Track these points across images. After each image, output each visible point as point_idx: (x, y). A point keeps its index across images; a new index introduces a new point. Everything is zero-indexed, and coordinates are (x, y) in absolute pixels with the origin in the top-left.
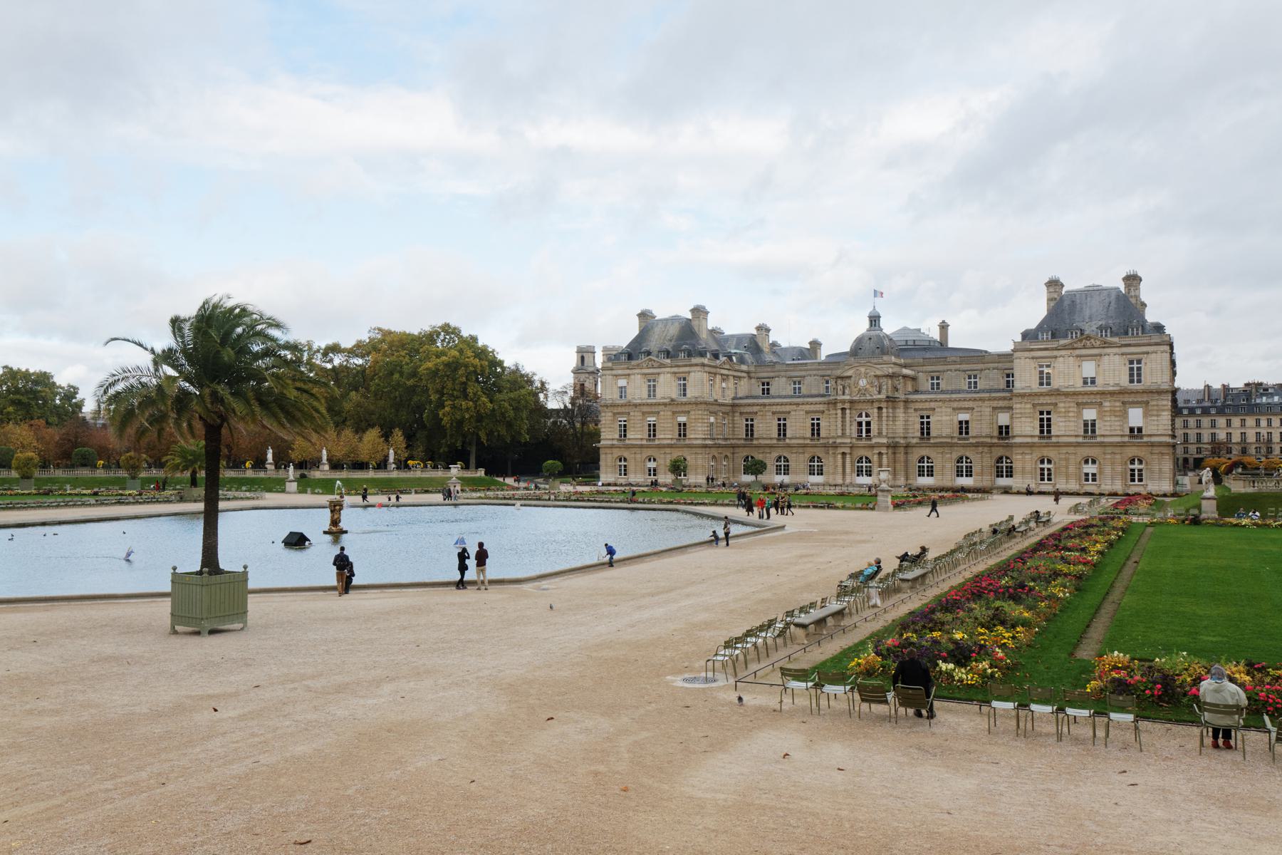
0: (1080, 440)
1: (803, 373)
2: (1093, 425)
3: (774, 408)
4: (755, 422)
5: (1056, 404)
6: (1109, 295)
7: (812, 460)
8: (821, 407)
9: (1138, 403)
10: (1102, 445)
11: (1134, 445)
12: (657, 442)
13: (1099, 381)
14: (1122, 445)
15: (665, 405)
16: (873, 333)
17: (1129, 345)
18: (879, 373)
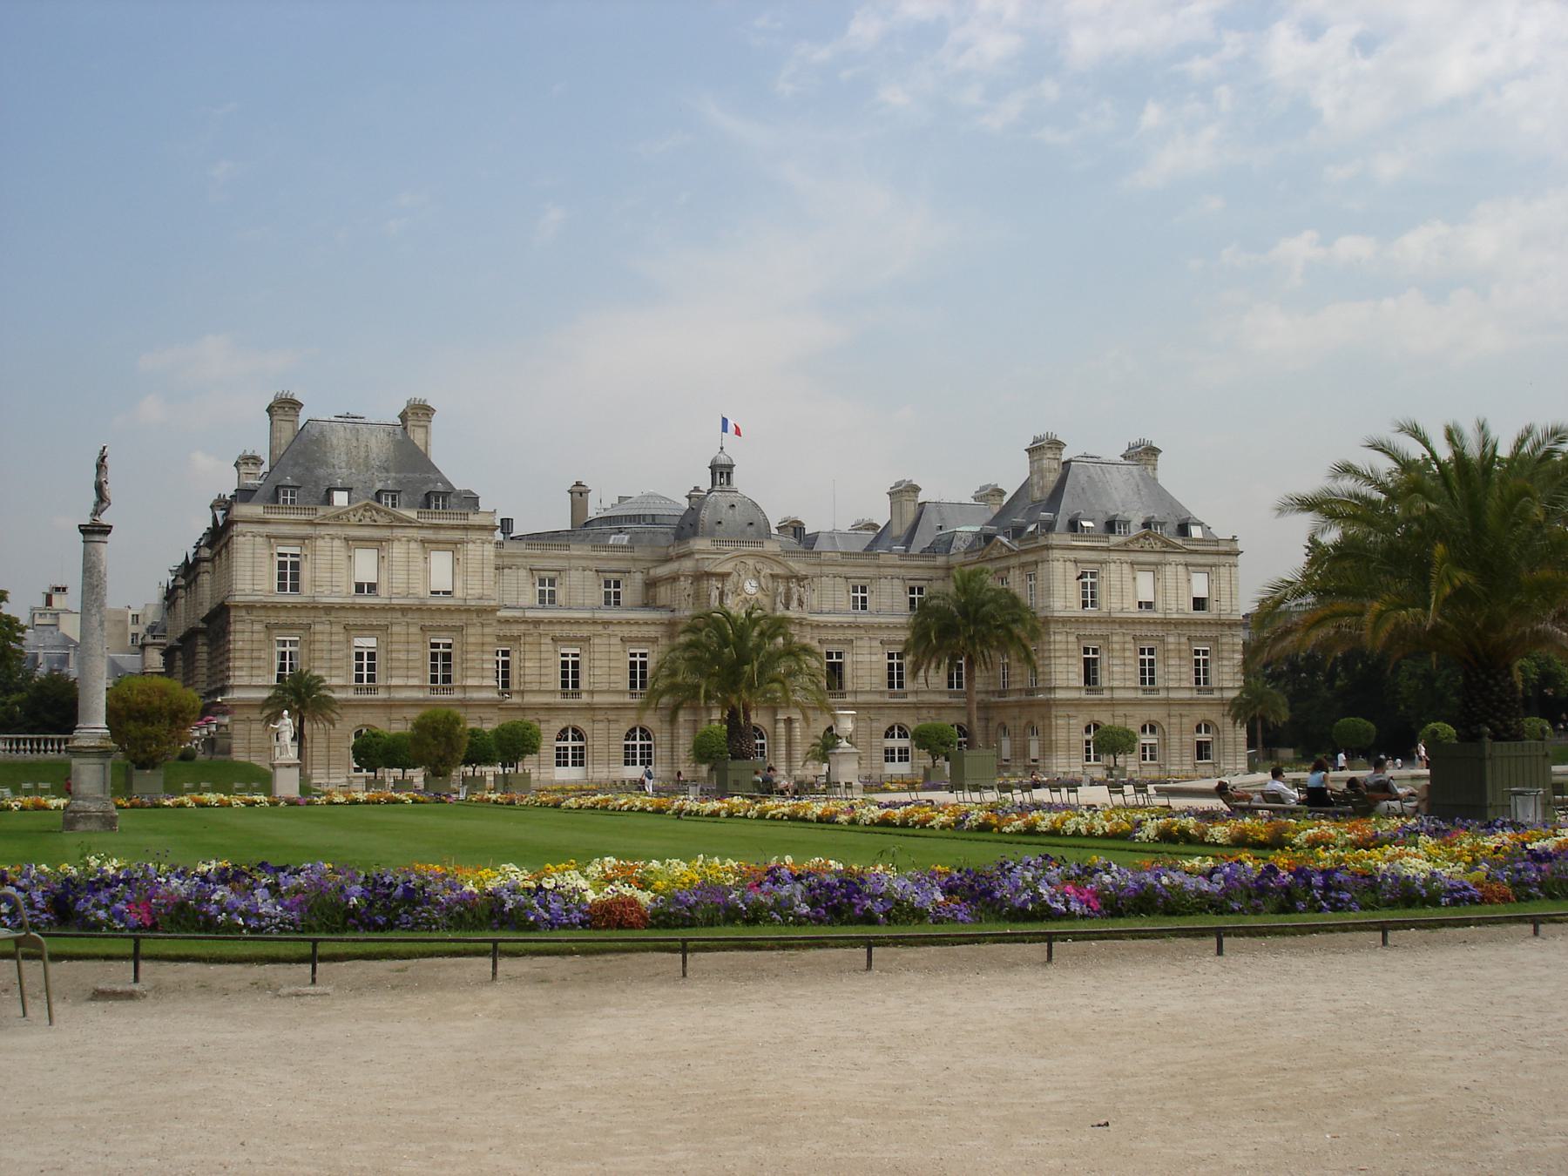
0: (1140, 695)
1: (565, 564)
2: (1152, 672)
3: (558, 631)
4: (514, 659)
5: (1106, 638)
6: (1130, 473)
7: (630, 735)
8: (652, 632)
9: (1206, 639)
10: (1168, 703)
11: (1207, 703)
12: (382, 695)
13: (1159, 605)
14: (1189, 703)
15: (405, 610)
16: (731, 498)
17: (1196, 552)
18: (778, 570)
